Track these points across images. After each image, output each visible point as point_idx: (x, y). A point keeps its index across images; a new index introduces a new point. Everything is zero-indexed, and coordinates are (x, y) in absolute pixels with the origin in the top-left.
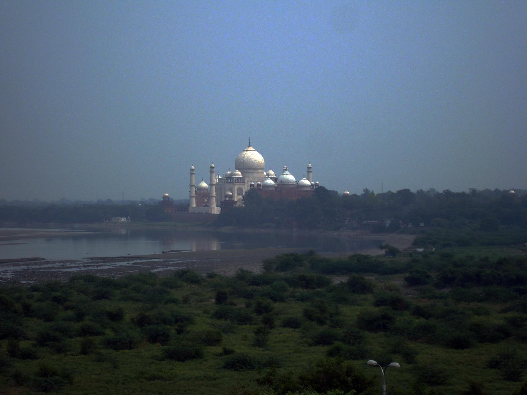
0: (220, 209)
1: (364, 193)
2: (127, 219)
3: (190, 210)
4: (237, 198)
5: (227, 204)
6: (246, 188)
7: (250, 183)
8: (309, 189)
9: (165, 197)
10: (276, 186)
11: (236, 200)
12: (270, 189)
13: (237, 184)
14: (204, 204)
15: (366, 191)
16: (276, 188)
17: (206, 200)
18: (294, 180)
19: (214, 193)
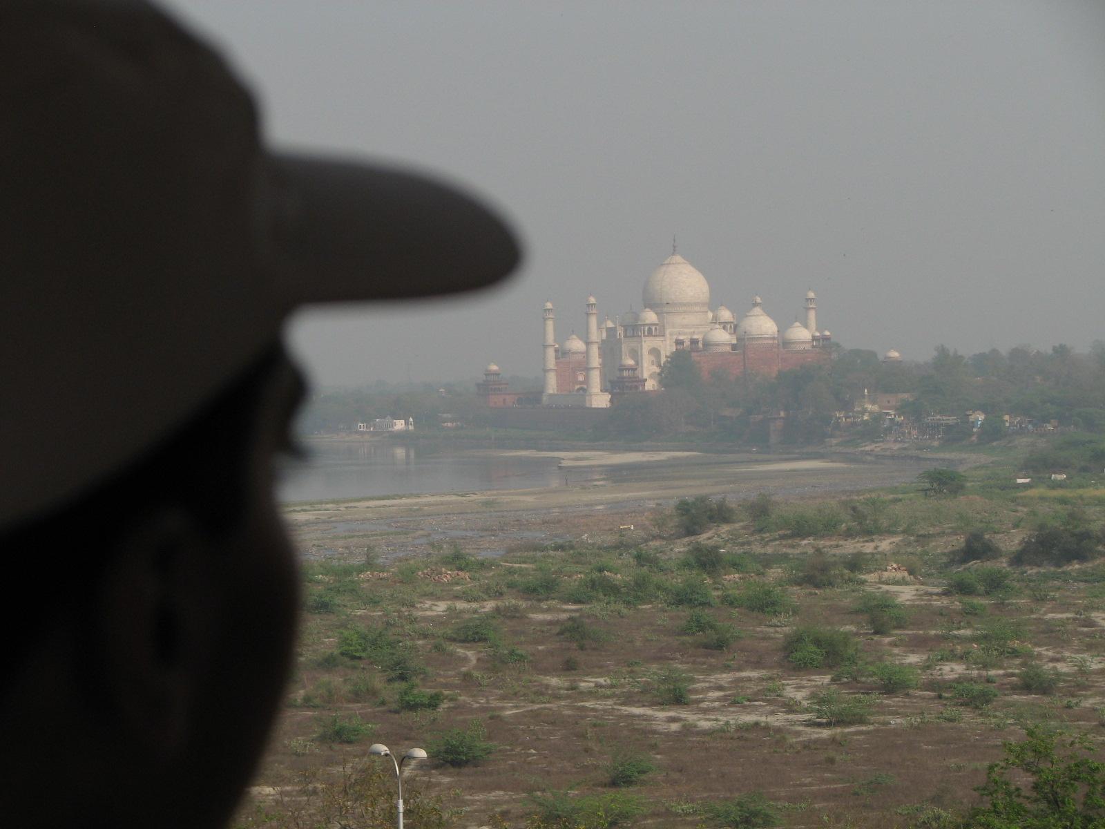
0: (607, 397)
1: (935, 353)
2: (407, 423)
3: (545, 398)
4: (649, 373)
5: (622, 384)
6: (668, 347)
7: (675, 337)
8: (808, 347)
9: (488, 373)
10: (734, 342)
11: (646, 375)
12: (720, 349)
13: (648, 339)
14: (577, 387)
15: (943, 351)
16: (734, 347)
17: (581, 378)
18: (775, 329)
19: (596, 361)
